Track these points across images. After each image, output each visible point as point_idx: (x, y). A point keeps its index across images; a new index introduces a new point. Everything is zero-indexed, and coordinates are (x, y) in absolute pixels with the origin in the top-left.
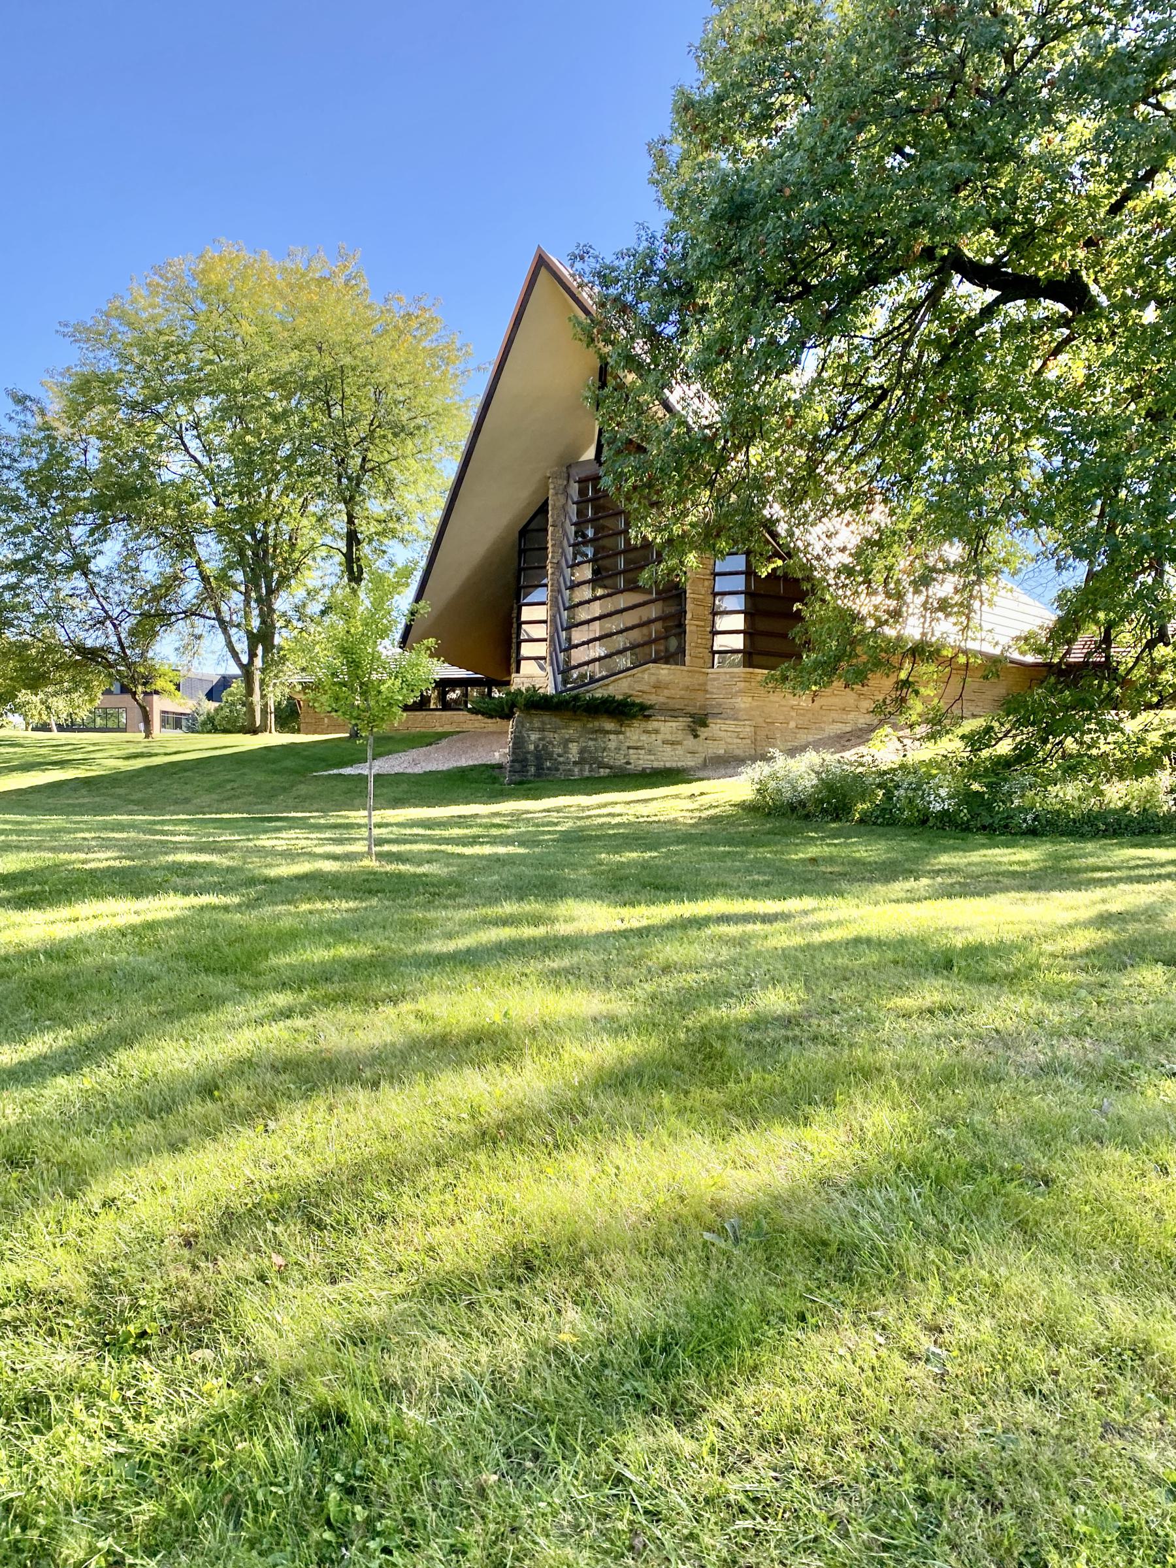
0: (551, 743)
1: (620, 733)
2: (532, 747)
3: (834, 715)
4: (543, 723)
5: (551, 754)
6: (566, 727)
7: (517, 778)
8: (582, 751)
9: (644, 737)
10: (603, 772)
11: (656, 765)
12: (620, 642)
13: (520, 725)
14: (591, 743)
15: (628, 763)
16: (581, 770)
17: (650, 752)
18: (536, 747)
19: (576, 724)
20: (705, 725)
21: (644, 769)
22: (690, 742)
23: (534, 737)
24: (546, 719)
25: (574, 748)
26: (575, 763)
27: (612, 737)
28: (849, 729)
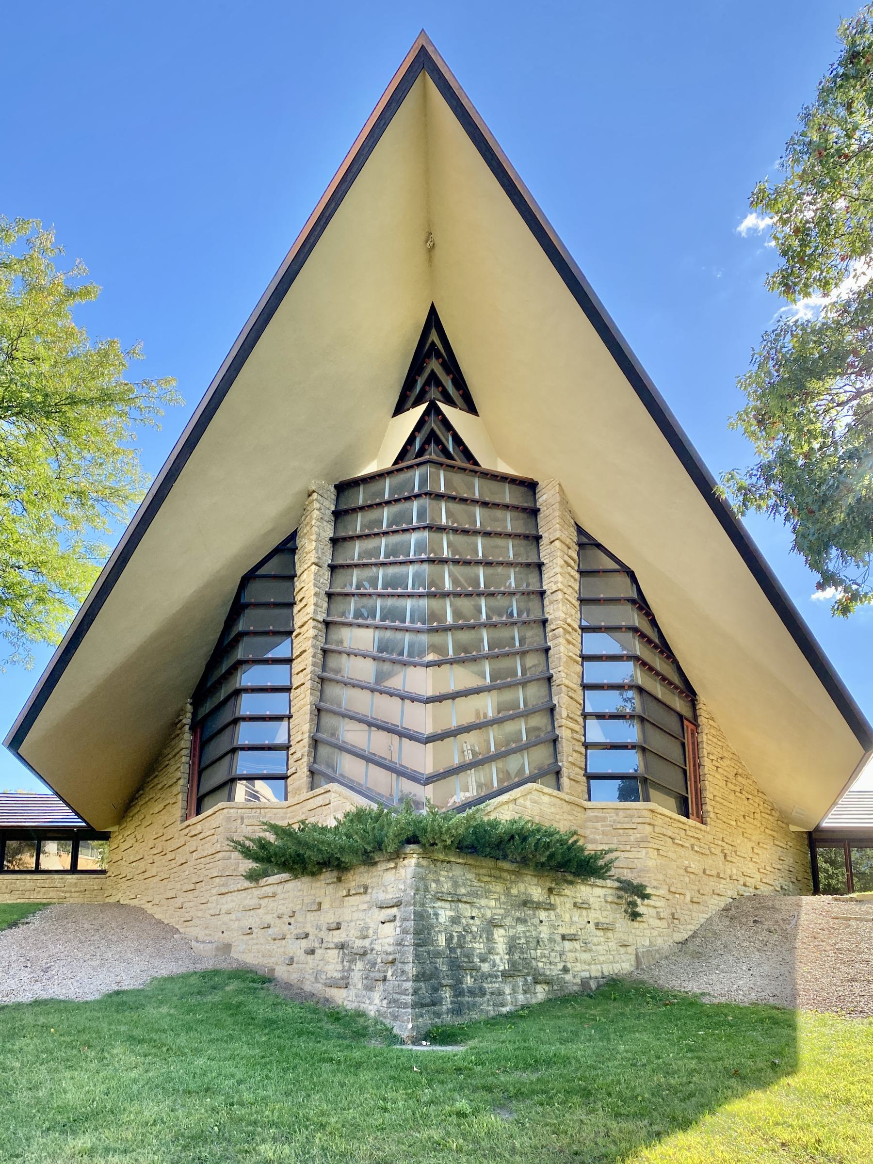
0: (467, 929)
1: (551, 907)
2: (442, 940)
3: (712, 883)
4: (456, 884)
5: (469, 956)
6: (487, 893)
7: (426, 1021)
8: (512, 947)
9: (576, 915)
10: (541, 993)
11: (595, 971)
12: (493, 737)
13: (421, 883)
14: (521, 928)
15: (565, 970)
16: (514, 991)
17: (586, 947)
18: (449, 939)
19: (498, 888)
20: (639, 892)
21: (585, 983)
22: (622, 923)
23: (445, 913)
24: (457, 871)
25: (499, 936)
26: (505, 975)
27: (543, 915)
28: (722, 905)
